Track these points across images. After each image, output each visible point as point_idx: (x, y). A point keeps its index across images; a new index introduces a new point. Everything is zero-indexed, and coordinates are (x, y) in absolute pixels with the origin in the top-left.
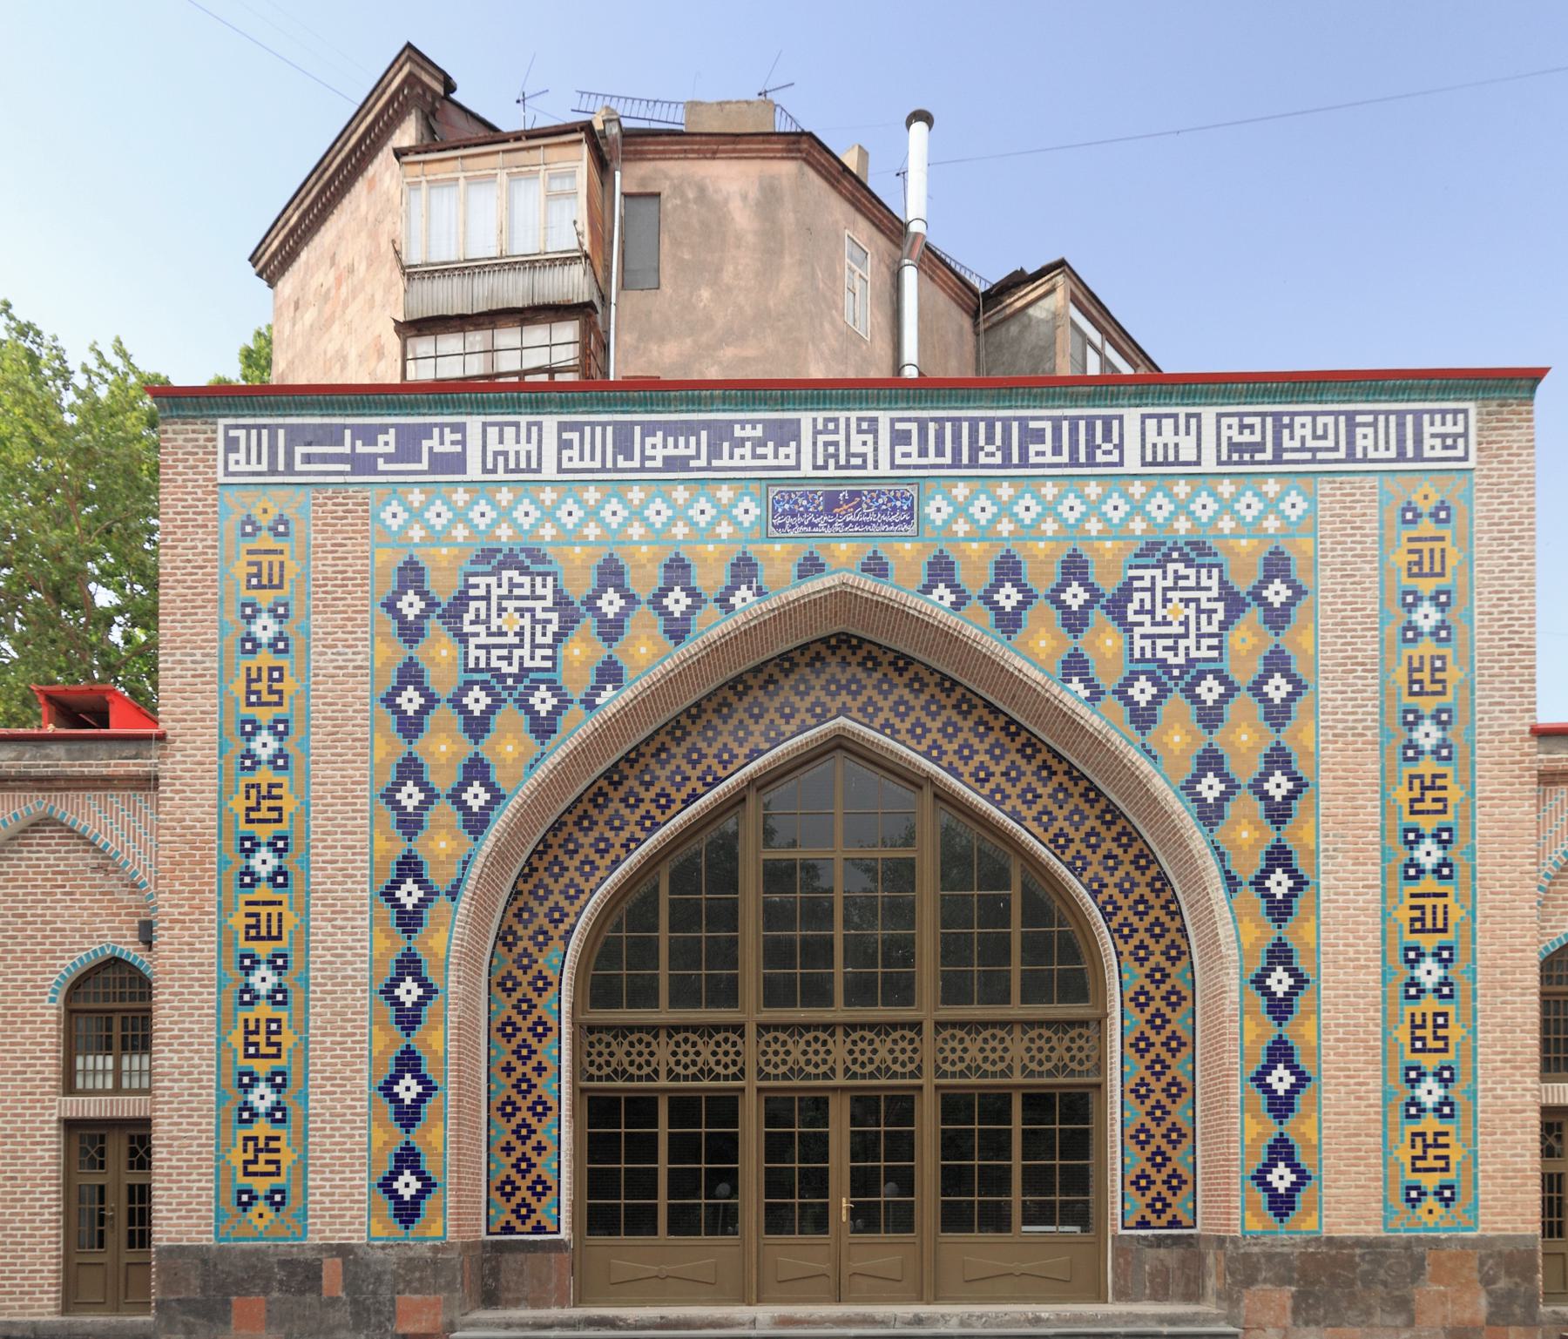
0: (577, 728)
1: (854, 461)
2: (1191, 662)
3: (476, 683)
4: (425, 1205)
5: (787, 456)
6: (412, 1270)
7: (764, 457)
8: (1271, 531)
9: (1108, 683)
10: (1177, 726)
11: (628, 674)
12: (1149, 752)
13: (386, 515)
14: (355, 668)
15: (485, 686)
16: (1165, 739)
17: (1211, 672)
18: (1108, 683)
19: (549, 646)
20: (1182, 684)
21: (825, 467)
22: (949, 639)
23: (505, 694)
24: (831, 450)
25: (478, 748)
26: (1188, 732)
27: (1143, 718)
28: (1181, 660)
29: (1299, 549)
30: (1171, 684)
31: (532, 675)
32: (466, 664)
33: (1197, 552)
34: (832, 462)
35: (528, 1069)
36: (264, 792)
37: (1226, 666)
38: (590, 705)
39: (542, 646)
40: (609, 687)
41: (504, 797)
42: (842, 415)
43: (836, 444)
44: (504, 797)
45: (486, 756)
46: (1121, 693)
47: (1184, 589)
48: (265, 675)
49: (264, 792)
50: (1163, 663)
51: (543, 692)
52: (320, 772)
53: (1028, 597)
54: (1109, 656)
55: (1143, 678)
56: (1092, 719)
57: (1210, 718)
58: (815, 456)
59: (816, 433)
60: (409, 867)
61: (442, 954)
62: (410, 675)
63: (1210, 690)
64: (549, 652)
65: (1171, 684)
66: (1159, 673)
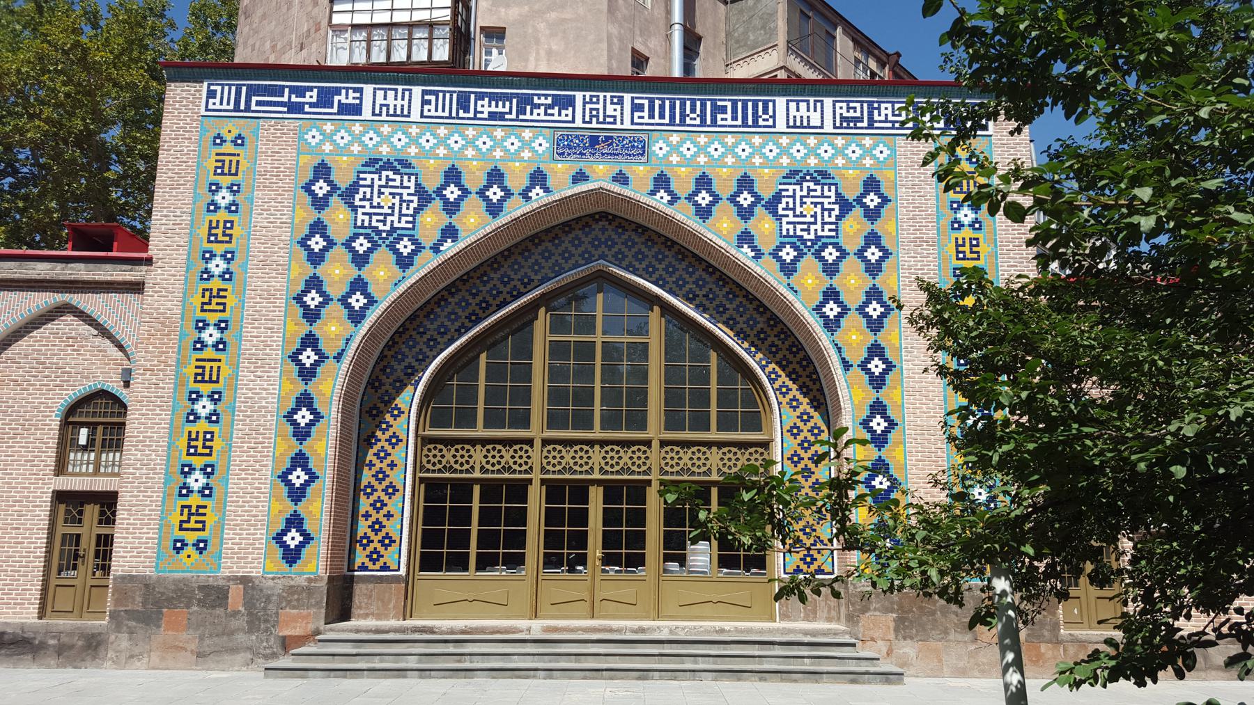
0: (427, 263)
1: (608, 120)
2: (818, 238)
3: (362, 234)
4: (304, 551)
5: (567, 115)
6: (293, 594)
7: (553, 115)
8: (868, 166)
9: (766, 249)
10: (810, 274)
11: (461, 234)
12: (792, 288)
13: (308, 137)
14: (281, 223)
15: (367, 237)
16: (802, 281)
17: (831, 244)
18: (766, 249)
19: (411, 215)
20: (813, 250)
21: (590, 122)
22: (668, 220)
23: (380, 242)
24: (594, 113)
25: (360, 273)
26: (817, 278)
27: (788, 269)
28: (812, 236)
29: (885, 177)
30: (806, 250)
31: (399, 232)
32: (355, 224)
33: (822, 176)
34: (594, 120)
35: (384, 465)
36: (215, 293)
37: (841, 241)
38: (436, 249)
39: (406, 215)
40: (449, 240)
41: (376, 302)
42: (601, 95)
43: (597, 110)
44: (376, 302)
45: (366, 278)
46: (775, 254)
47: (813, 197)
48: (221, 225)
49: (215, 293)
50: (801, 238)
51: (406, 241)
52: (253, 283)
53: (716, 199)
54: (767, 233)
55: (788, 246)
56: (757, 268)
57: (831, 270)
58: (584, 116)
59: (585, 103)
60: (310, 341)
61: (328, 394)
62: (318, 228)
63: (830, 254)
64: (411, 219)
65: (806, 250)
66: (799, 245)
